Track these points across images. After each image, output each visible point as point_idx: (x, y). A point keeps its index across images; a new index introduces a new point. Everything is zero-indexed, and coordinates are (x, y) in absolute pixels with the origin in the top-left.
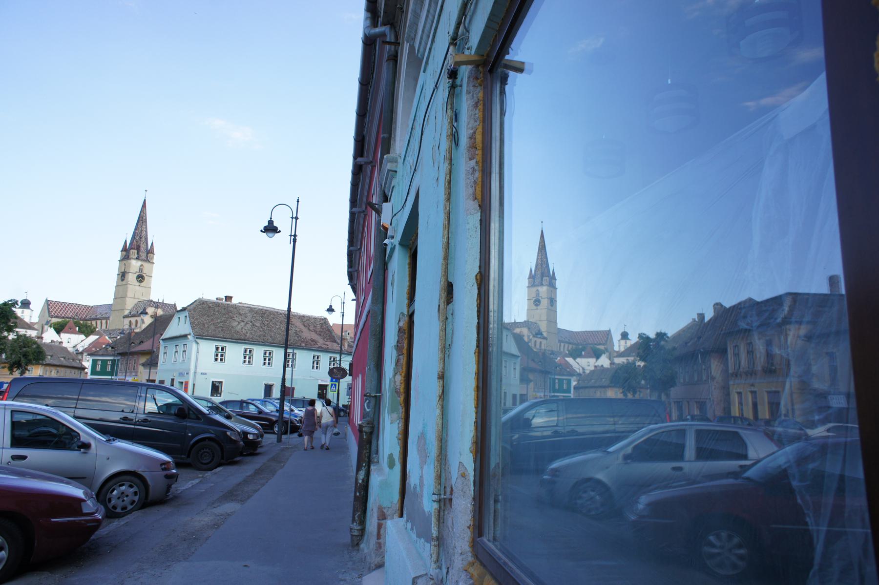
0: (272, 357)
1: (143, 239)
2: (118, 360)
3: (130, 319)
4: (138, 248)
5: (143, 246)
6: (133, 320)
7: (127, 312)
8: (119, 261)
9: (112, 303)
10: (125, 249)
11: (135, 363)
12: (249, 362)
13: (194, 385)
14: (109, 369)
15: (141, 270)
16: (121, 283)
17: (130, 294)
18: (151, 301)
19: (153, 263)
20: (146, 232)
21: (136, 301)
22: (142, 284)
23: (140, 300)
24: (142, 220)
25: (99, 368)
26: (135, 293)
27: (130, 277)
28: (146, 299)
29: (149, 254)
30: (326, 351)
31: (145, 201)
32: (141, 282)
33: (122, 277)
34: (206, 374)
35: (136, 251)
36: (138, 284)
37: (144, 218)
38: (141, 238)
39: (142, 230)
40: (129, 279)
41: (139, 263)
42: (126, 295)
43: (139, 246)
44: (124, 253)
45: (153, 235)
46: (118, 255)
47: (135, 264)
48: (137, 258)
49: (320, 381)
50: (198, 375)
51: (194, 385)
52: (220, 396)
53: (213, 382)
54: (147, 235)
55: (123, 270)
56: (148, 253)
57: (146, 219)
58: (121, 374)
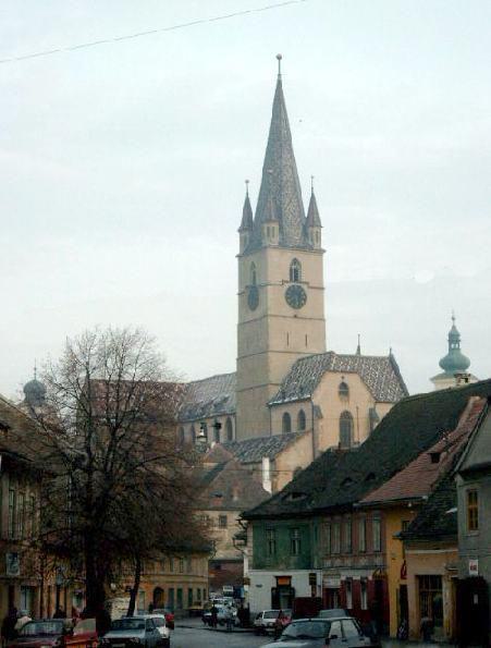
1: (289, 191)
3: (284, 410)
5: (289, 209)
15: (295, 274)
16: (251, 316)
17: (276, 342)
18: (331, 353)
21: (293, 359)
22: (304, 311)
23: (300, 356)
27: (270, 296)
36: (289, 311)
40: (269, 303)
41: (288, 257)
42: (268, 346)
44: (247, 234)
46: (234, 245)
55: (249, 283)
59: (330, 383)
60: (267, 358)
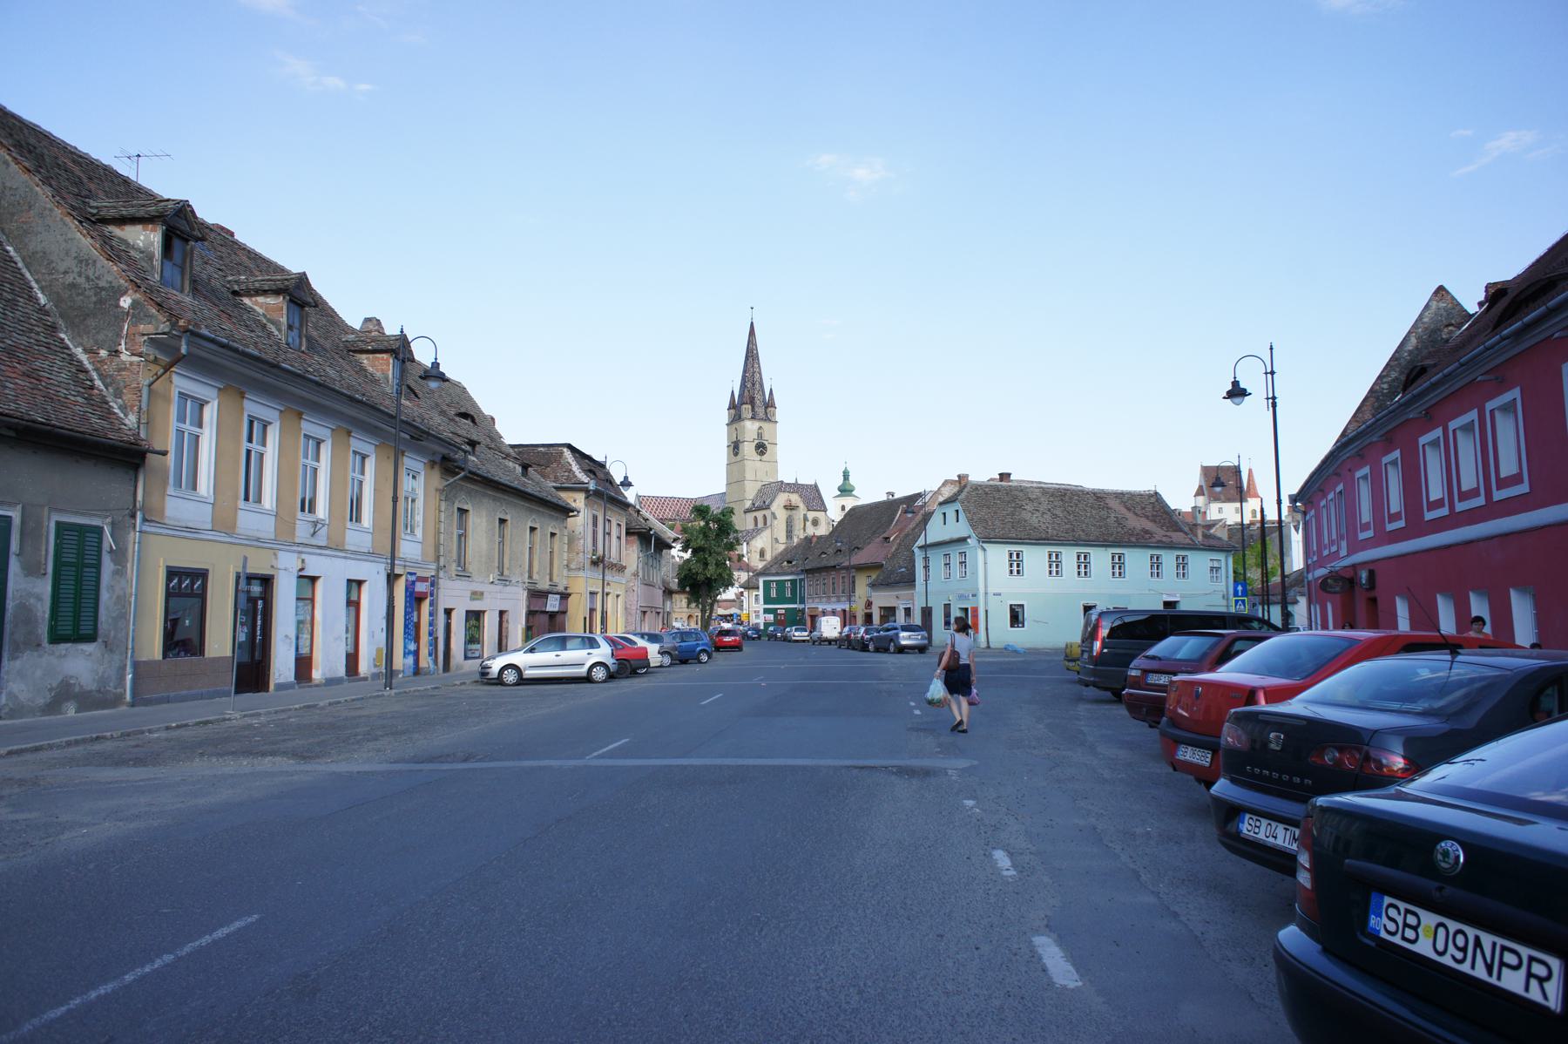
0: (1022, 561)
1: (757, 386)
2: (801, 580)
4: (752, 402)
5: (758, 397)
6: (759, 515)
7: (748, 504)
8: (727, 425)
9: (724, 491)
10: (733, 406)
11: (833, 584)
12: (1018, 572)
13: (987, 611)
14: (788, 594)
15: (760, 435)
16: (734, 459)
17: (749, 475)
18: (782, 482)
19: (776, 422)
20: (760, 374)
21: (760, 484)
22: (764, 458)
23: (764, 483)
24: (751, 356)
25: (774, 594)
26: (756, 473)
27: (746, 449)
28: (773, 481)
29: (769, 409)
30: (1171, 546)
31: (752, 323)
32: (762, 454)
33: (734, 449)
34: (1000, 595)
35: (750, 407)
36: (759, 457)
37: (755, 352)
38: (753, 385)
39: (754, 373)
41: (757, 424)
43: (754, 398)
44: (733, 411)
45: (771, 377)
46: (724, 416)
47: (750, 427)
48: (752, 418)
49: (1164, 596)
50: (990, 597)
51: (987, 611)
52: (1023, 627)
53: (1011, 605)
54: (761, 379)
56: (766, 408)
57: (757, 353)
58: (810, 601)
59: (782, 499)
60: (744, 484)
